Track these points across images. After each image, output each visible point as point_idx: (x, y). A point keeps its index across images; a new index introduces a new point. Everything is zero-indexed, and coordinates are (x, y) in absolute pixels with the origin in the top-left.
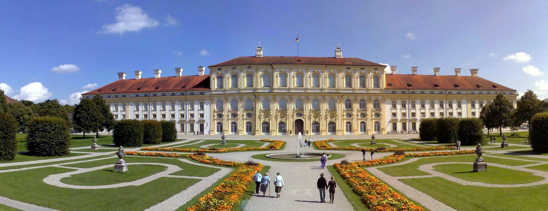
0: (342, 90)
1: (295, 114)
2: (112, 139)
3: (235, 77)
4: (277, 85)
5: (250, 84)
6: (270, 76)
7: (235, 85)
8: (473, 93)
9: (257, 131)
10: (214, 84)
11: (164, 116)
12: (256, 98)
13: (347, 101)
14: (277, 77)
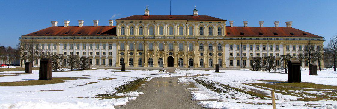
0: (197, 37)
1: (168, 53)
2: (39, 68)
3: (132, 28)
4: (157, 33)
5: (141, 34)
6: (153, 28)
7: (132, 34)
9: (145, 64)
10: (119, 32)
11: (85, 53)
12: (144, 42)
13: (200, 44)
14: (158, 28)
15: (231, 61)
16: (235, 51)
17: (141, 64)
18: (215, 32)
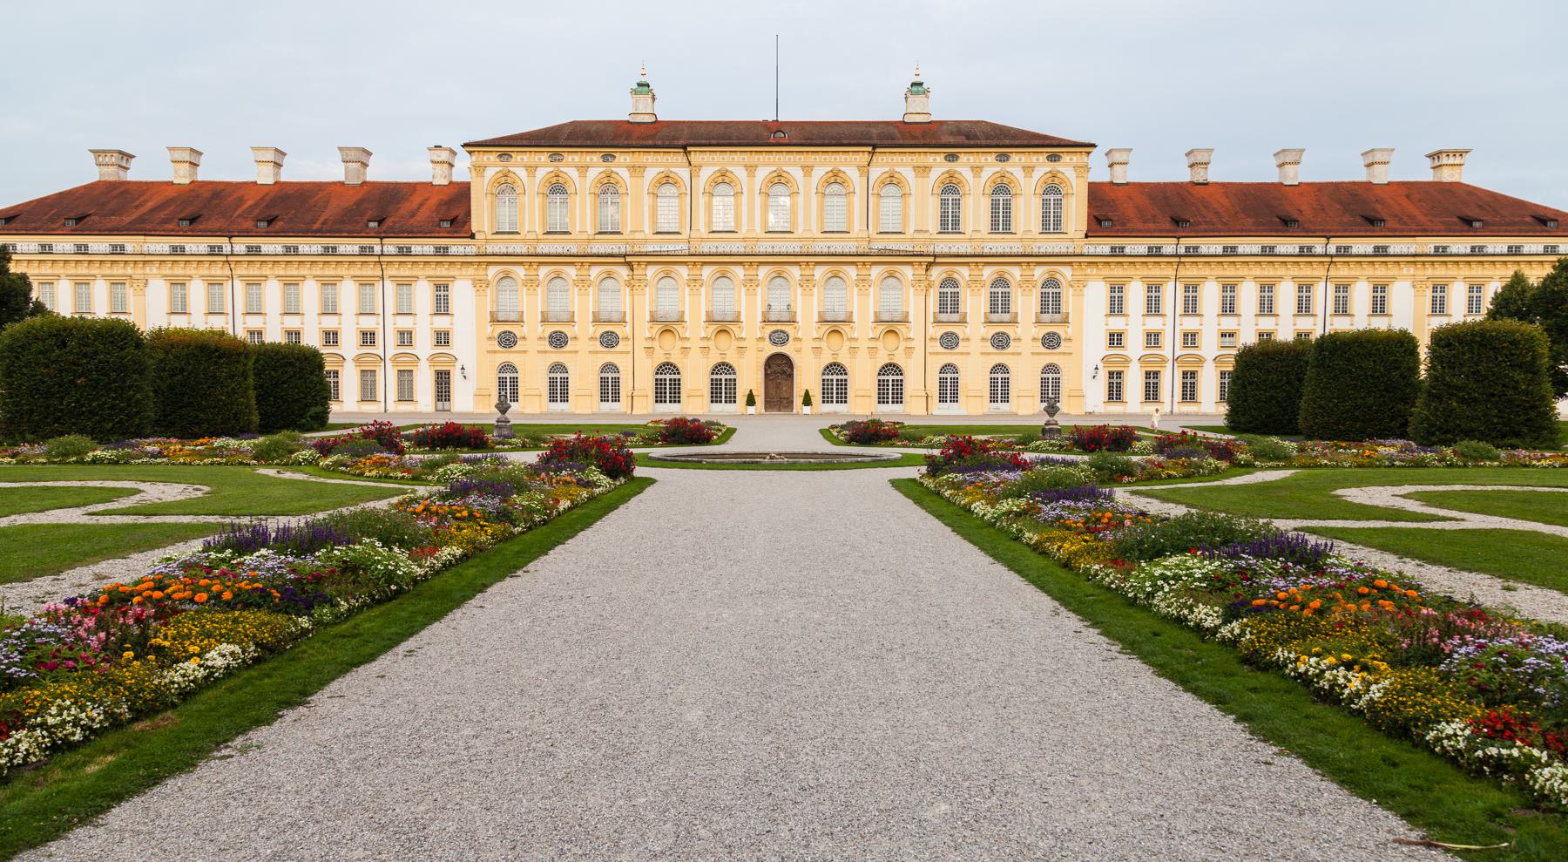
15: (1111, 374)
18: (1027, 213)
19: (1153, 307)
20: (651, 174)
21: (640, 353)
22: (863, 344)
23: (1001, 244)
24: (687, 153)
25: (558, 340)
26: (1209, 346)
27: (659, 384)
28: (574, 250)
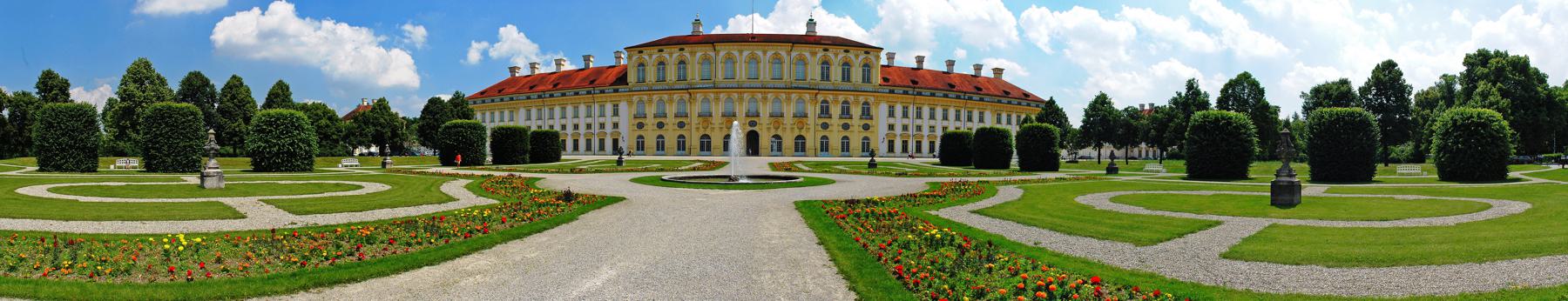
6: (710, 63)
8: (999, 102)
15: (889, 141)
16: (898, 122)
17: (684, 149)
19: (905, 115)
20: (699, 54)
21: (693, 130)
22: (788, 127)
23: (846, 86)
24: (714, 47)
25: (660, 125)
26: (939, 133)
27: (702, 144)
28: (667, 88)
